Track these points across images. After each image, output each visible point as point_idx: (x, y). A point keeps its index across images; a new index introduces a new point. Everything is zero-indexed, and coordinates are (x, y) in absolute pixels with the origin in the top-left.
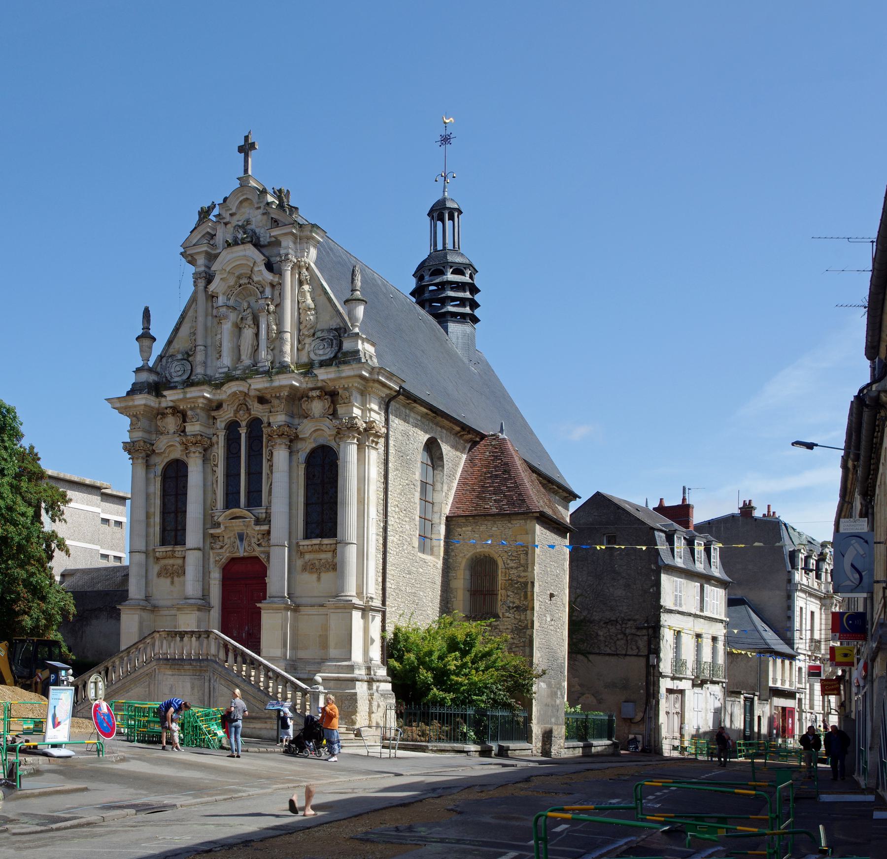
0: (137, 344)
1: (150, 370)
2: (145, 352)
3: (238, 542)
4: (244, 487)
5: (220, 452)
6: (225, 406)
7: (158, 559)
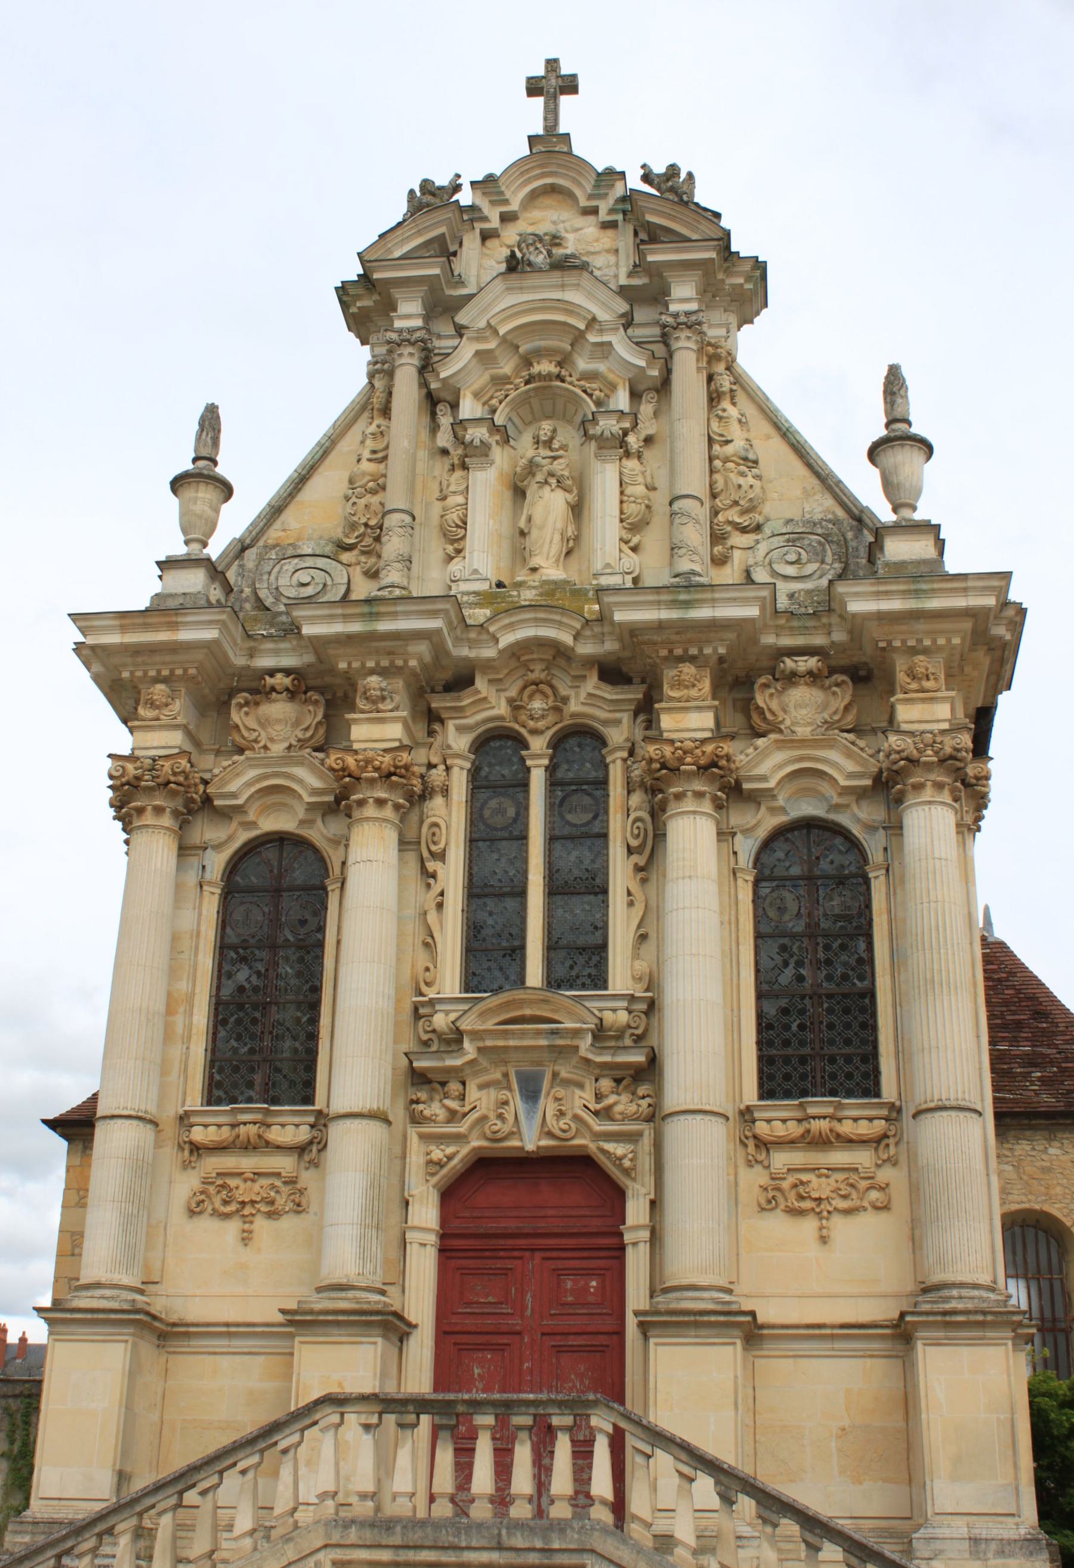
1: (215, 571)
2: (198, 529)
3: (517, 1102)
4: (537, 934)
5: (451, 816)
6: (480, 683)
7: (196, 1149)
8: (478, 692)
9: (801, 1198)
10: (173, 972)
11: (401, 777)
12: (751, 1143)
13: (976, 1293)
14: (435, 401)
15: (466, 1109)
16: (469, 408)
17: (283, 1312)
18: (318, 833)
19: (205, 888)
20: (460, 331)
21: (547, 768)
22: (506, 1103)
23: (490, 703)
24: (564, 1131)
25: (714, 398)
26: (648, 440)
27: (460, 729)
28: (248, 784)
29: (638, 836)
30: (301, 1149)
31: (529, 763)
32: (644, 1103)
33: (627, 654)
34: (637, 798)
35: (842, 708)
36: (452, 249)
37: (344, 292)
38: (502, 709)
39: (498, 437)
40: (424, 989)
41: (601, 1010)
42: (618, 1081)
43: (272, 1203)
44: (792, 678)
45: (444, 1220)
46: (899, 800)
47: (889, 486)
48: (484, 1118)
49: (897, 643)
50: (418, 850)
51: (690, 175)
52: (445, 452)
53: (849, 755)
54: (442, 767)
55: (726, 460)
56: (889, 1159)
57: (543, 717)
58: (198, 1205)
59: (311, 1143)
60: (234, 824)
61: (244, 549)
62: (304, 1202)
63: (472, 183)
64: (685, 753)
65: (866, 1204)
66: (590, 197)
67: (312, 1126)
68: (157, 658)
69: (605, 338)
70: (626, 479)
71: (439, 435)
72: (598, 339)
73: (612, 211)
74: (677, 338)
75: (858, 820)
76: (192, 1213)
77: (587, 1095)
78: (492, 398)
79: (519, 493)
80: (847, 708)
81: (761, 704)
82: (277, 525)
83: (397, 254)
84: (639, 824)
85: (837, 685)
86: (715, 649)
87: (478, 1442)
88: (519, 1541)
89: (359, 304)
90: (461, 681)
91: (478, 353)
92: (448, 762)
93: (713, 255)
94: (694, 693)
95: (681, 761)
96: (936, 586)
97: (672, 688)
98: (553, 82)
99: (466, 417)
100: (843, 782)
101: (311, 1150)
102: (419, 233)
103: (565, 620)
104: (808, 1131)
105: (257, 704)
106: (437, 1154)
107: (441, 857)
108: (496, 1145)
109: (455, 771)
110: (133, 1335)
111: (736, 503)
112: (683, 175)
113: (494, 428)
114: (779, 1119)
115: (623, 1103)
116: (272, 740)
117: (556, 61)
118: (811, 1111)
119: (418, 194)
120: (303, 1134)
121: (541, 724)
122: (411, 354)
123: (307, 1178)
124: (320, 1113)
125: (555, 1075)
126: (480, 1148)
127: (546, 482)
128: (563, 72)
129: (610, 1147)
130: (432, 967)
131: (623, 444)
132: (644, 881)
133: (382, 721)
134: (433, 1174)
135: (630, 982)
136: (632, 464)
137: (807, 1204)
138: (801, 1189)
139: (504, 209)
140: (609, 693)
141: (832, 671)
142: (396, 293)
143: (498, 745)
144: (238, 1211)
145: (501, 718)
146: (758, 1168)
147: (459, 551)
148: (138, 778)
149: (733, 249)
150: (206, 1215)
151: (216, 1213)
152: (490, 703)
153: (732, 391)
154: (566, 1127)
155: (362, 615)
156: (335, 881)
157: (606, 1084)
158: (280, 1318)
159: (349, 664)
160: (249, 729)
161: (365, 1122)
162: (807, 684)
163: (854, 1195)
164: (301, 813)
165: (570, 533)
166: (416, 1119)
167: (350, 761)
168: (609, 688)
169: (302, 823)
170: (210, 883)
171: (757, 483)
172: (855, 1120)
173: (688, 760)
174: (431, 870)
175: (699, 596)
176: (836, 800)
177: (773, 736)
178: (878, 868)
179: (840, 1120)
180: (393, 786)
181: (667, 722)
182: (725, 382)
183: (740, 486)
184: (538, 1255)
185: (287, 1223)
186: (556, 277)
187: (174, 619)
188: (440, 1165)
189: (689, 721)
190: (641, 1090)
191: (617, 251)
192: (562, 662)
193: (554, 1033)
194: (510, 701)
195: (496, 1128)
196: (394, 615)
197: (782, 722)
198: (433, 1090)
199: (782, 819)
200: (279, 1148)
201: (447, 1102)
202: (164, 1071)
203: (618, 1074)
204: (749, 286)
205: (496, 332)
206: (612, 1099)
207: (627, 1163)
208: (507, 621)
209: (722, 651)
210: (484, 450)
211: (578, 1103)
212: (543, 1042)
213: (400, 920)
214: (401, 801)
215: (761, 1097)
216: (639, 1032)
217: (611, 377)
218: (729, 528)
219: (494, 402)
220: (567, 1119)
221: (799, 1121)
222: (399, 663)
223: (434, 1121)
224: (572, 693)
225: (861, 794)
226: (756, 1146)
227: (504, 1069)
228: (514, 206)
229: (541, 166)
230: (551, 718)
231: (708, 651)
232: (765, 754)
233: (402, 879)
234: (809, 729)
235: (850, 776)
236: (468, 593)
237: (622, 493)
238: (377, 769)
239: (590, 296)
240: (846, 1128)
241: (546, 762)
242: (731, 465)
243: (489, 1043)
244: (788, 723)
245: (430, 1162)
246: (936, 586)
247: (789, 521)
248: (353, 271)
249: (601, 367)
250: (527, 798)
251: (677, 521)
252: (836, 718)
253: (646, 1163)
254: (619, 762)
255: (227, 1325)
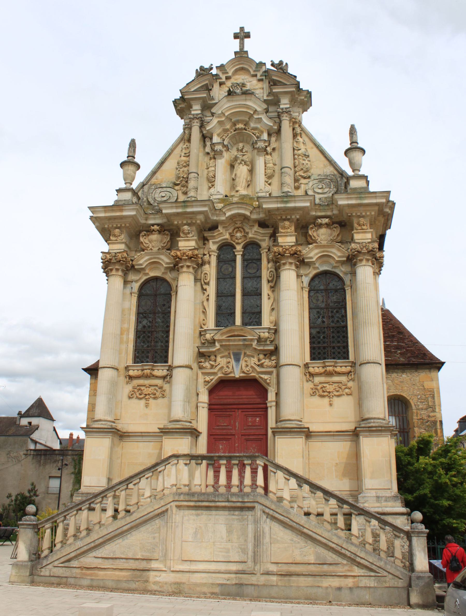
0: (120, 171)
1: (135, 193)
2: (129, 179)
3: (233, 362)
5: (211, 270)
6: (220, 228)
7: (131, 378)
8: (219, 231)
9: (324, 392)
10: (122, 321)
11: (195, 258)
12: (308, 375)
13: (379, 421)
14: (205, 137)
15: (217, 364)
16: (216, 139)
17: (159, 428)
18: (169, 277)
19: (132, 294)
20: (213, 114)
21: (242, 255)
22: (229, 362)
23: (223, 234)
24: (248, 371)
25: (295, 136)
26: (274, 149)
27: (214, 243)
28: (146, 261)
29: (271, 277)
30: (164, 378)
31: (236, 253)
32: (274, 362)
33: (267, 218)
34: (270, 265)
35: (337, 235)
36: (210, 88)
37: (175, 102)
38: (227, 236)
39: (225, 149)
40: (203, 326)
41: (259, 333)
42: (265, 355)
43: (155, 394)
44: (320, 226)
45: (210, 400)
46: (355, 265)
47: (351, 164)
48: (222, 367)
49: (354, 214)
50: (201, 282)
51: (287, 64)
52: (208, 153)
53: (339, 250)
54: (208, 255)
55: (299, 155)
56: (351, 379)
57: (240, 239)
58: (131, 395)
59: (167, 375)
60: (142, 274)
61: (144, 185)
62: (165, 394)
63: (216, 67)
64: (286, 250)
65: (344, 393)
66: (254, 71)
67: (168, 370)
68: (116, 221)
69: (260, 117)
70: (267, 162)
71: (206, 148)
72: (257, 117)
73: (261, 76)
74: (283, 116)
75: (342, 271)
76: (130, 398)
77: (255, 360)
78: (223, 136)
79: (232, 167)
80: (338, 235)
81: (310, 234)
82: (154, 177)
83: (192, 90)
84: (271, 273)
85: (335, 228)
86: (296, 216)
87: (221, 469)
88: (234, 499)
89: (180, 106)
90: (214, 227)
91: (218, 122)
92: (210, 253)
93: (294, 89)
94: (289, 230)
95: (285, 252)
96: (366, 196)
97: (282, 229)
98: (242, 34)
99: (215, 142)
100: (337, 259)
101: (168, 378)
102: (199, 83)
103: (247, 207)
104: (326, 370)
105: (148, 235)
106: (208, 379)
107: (208, 284)
108: (226, 376)
109: (212, 256)
110: (112, 436)
111: (302, 169)
112: (284, 64)
113: (224, 146)
114: (317, 367)
115: (267, 362)
116: (153, 247)
117: (243, 28)
118: (327, 364)
119: (199, 71)
120: (165, 373)
121: (240, 241)
122: (197, 122)
123: (166, 387)
124: (170, 366)
125: (245, 353)
126: (221, 377)
127: (241, 163)
128: (245, 31)
129: (263, 376)
130: (205, 319)
131: (265, 150)
132: (273, 291)
133: (189, 240)
134: (206, 385)
135: (269, 324)
136: (268, 157)
137: (326, 394)
138: (324, 389)
139: (227, 75)
140: (261, 231)
141: (333, 223)
142: (192, 103)
143: (226, 248)
144: (144, 397)
145: (227, 239)
146: (310, 382)
147: (213, 185)
148: (111, 259)
149: (301, 87)
150: (134, 398)
151: (137, 398)
152: (223, 234)
153: (300, 133)
154: (248, 370)
155: (182, 206)
156: (174, 292)
157: (261, 356)
158: (158, 431)
159: (178, 222)
160: (146, 243)
161: (184, 369)
162: (325, 227)
163: (341, 390)
164: (163, 270)
165: (249, 179)
166: (201, 368)
167: (179, 253)
168: (262, 229)
169: (163, 273)
170: (134, 293)
171: (309, 163)
172: (341, 367)
173: (287, 252)
174: (205, 288)
175: (290, 199)
176: (335, 265)
177: (314, 244)
178: (348, 286)
179: (336, 367)
180: (192, 261)
181: (280, 240)
182: (298, 130)
183: (303, 164)
184: (240, 411)
185: (160, 401)
186: (243, 97)
187: (121, 208)
188: (208, 382)
189: (287, 240)
190: (273, 358)
191: (263, 88)
192: (247, 221)
193: (245, 340)
194: (230, 234)
195: (226, 370)
196: (192, 206)
197: (317, 240)
198: (206, 358)
199: (318, 271)
200: (157, 377)
201: (210, 362)
202: (120, 353)
203: (265, 353)
204: (306, 99)
205: (224, 115)
206: (263, 361)
207: (268, 381)
208: (228, 208)
209: (298, 217)
210: (221, 153)
211: (252, 362)
212: (241, 343)
213: (195, 304)
214: (195, 266)
215: (311, 360)
216: (272, 339)
217: (262, 129)
218: (300, 177)
219: (224, 137)
220: (249, 367)
221: (323, 367)
222: (194, 221)
223: (206, 368)
224: (249, 231)
225: (343, 263)
226: (310, 375)
227: (229, 352)
228: (230, 74)
229: (238, 61)
230: (243, 239)
231: (293, 217)
232: (312, 250)
233: (195, 291)
234: (326, 242)
235: (339, 257)
236: (216, 199)
237: (265, 166)
238: (187, 256)
239: (255, 103)
240: (338, 369)
241: (241, 253)
242: (300, 157)
243: (224, 343)
244: (319, 240)
245: (205, 381)
246: (366, 196)
247: (319, 175)
248: (178, 95)
249: (258, 126)
250: (235, 265)
251: (283, 175)
252: (335, 238)
253: (274, 381)
254: (265, 253)
255: (141, 433)
